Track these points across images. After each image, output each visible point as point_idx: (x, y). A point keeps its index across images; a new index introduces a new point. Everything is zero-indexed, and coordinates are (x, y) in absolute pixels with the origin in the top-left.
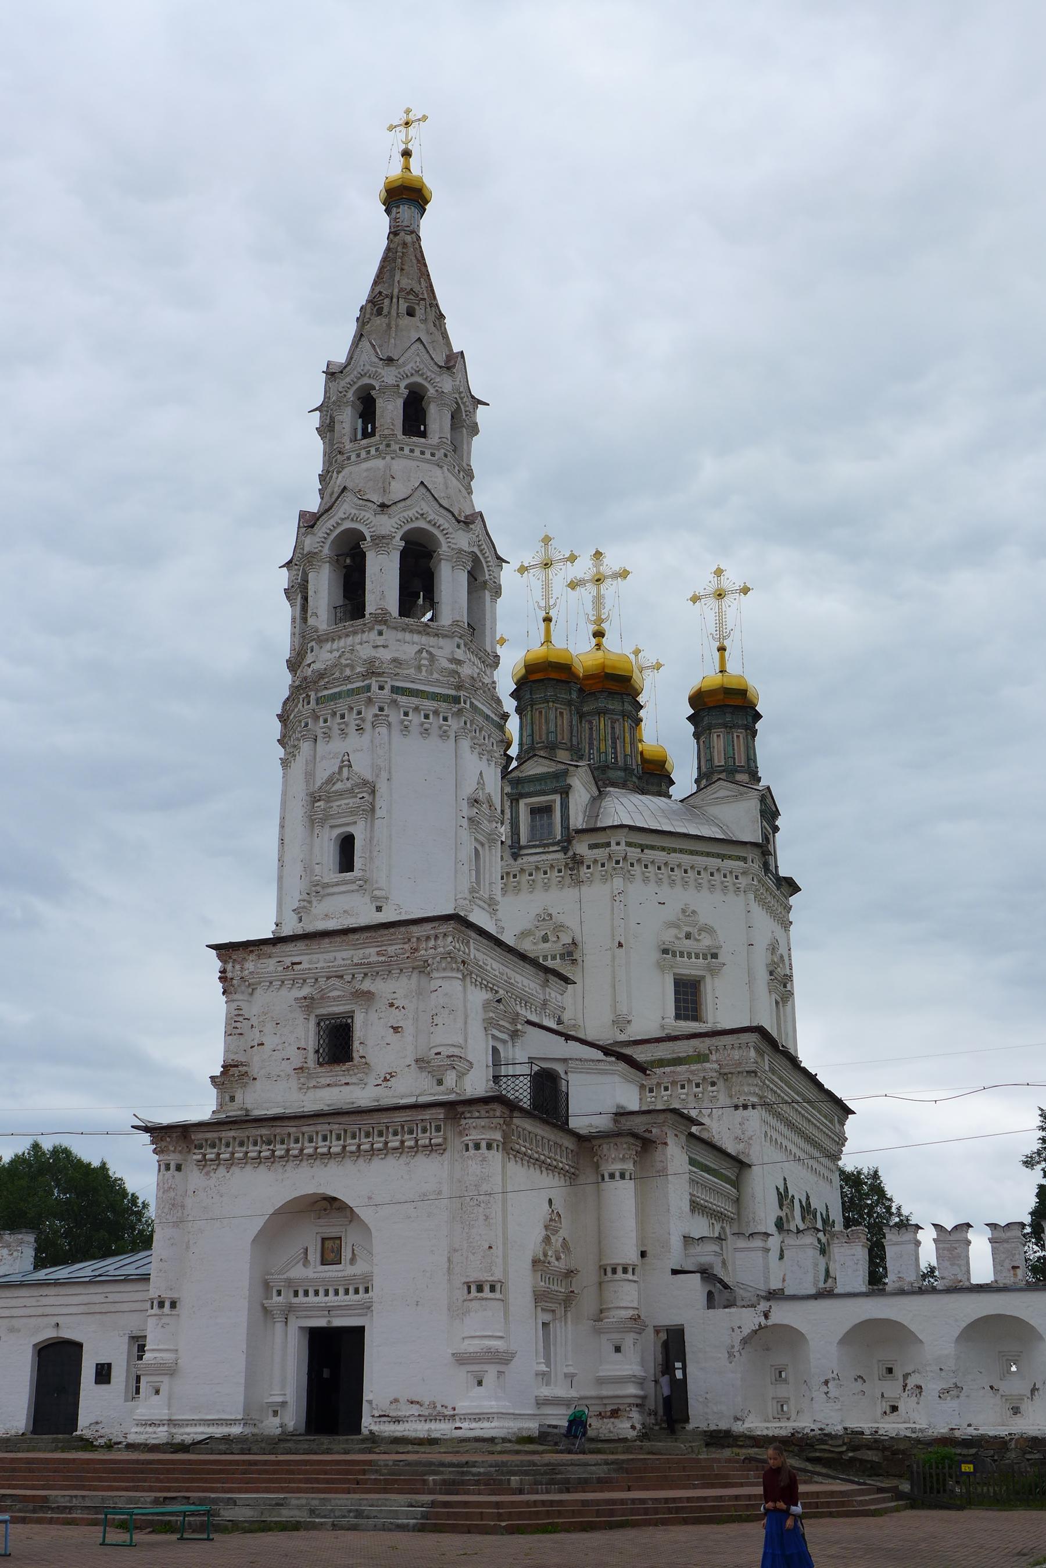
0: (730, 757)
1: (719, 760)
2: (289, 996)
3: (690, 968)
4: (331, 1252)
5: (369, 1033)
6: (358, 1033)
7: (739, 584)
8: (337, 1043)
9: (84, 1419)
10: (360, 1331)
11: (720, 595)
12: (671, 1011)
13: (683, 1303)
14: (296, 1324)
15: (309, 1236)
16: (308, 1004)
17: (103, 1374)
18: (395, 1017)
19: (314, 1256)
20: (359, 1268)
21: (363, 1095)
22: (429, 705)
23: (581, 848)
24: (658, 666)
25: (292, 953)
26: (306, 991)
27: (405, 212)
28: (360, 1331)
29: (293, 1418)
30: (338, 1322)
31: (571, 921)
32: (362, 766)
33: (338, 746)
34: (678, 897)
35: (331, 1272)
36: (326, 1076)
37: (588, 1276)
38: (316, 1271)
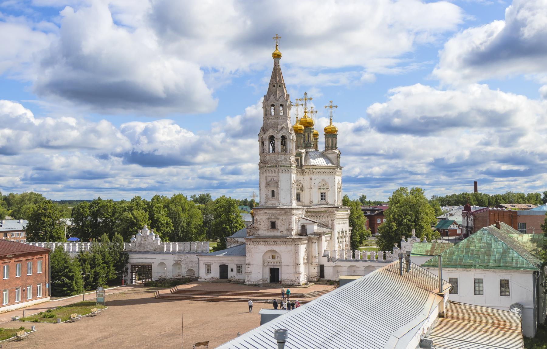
0: (332, 144)
1: (330, 145)
2: (264, 218)
3: (323, 191)
4: (274, 257)
5: (279, 224)
6: (277, 224)
7: (335, 105)
8: (273, 226)
9: (229, 276)
10: (278, 269)
11: (331, 107)
12: (320, 199)
13: (324, 261)
14: (269, 267)
15: (270, 254)
16: (268, 219)
17: (232, 270)
18: (283, 222)
19: (271, 258)
20: (279, 259)
21: (278, 234)
22: (286, 168)
23: (304, 168)
24: (316, 112)
25: (265, 211)
26: (268, 217)
27: (277, 59)
28: (278, 269)
29: (269, 281)
30: (275, 267)
31: (302, 182)
32: (275, 178)
33: (271, 175)
34: (322, 177)
35: (274, 260)
36: (272, 230)
37: (263, 185)
38: (271, 260)
